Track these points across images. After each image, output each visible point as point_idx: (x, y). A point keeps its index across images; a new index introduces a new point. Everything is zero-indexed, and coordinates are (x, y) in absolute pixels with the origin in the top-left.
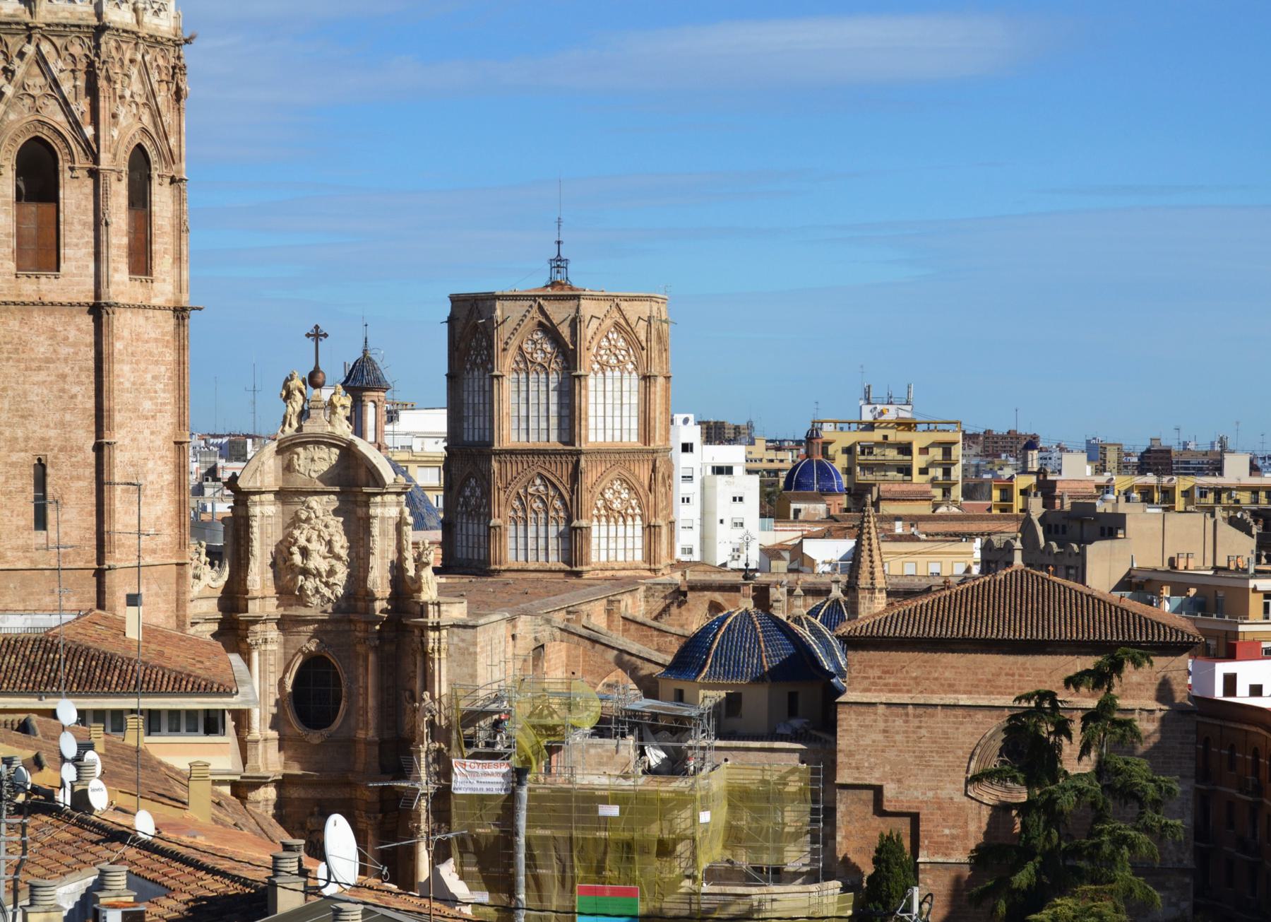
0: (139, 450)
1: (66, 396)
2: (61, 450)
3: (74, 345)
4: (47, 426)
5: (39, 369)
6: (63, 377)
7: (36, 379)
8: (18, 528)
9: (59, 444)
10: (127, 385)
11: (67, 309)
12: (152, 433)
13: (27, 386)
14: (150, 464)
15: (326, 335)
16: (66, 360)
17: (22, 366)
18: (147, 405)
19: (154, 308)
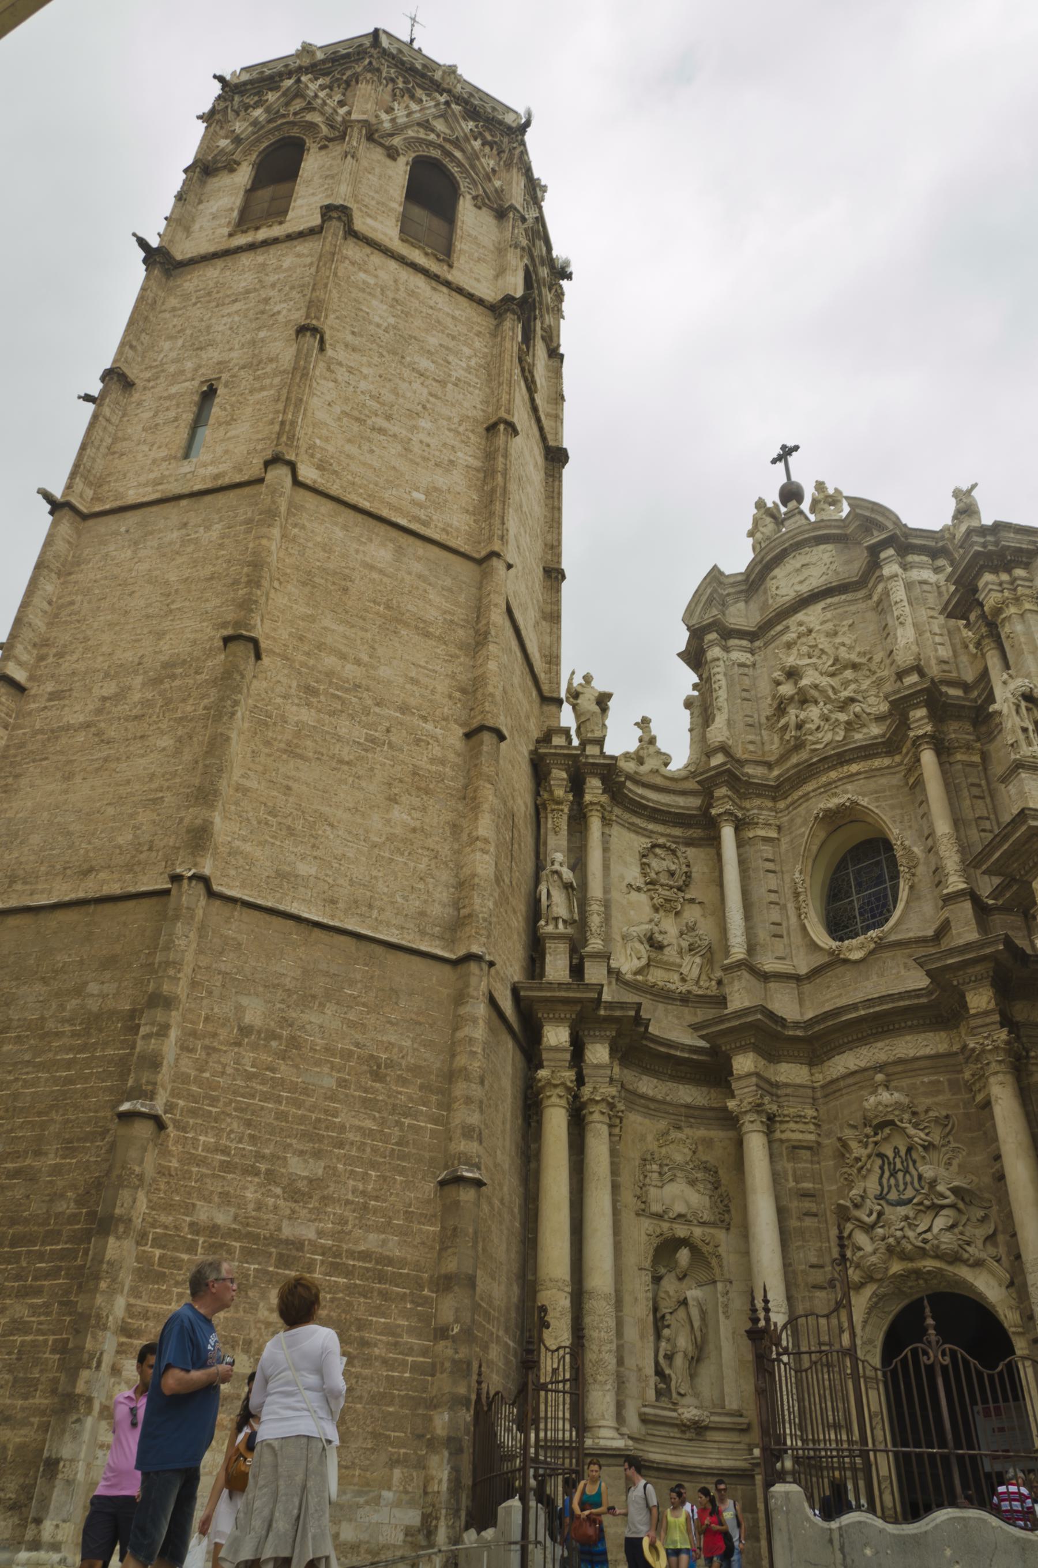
0: (395, 391)
1: (265, 316)
2: (243, 367)
3: (289, 269)
4: (231, 349)
5: (235, 301)
6: (267, 300)
7: (226, 311)
8: (154, 461)
9: (242, 362)
10: (377, 319)
11: (288, 244)
12: (431, 394)
13: (213, 321)
14: (424, 423)
15: (796, 448)
16: (273, 286)
17: (214, 304)
18: (424, 363)
19: (448, 284)
